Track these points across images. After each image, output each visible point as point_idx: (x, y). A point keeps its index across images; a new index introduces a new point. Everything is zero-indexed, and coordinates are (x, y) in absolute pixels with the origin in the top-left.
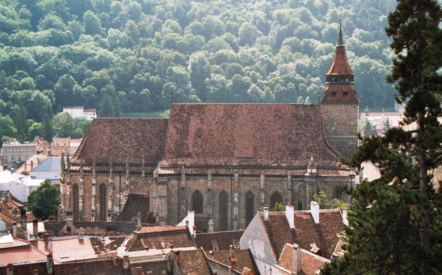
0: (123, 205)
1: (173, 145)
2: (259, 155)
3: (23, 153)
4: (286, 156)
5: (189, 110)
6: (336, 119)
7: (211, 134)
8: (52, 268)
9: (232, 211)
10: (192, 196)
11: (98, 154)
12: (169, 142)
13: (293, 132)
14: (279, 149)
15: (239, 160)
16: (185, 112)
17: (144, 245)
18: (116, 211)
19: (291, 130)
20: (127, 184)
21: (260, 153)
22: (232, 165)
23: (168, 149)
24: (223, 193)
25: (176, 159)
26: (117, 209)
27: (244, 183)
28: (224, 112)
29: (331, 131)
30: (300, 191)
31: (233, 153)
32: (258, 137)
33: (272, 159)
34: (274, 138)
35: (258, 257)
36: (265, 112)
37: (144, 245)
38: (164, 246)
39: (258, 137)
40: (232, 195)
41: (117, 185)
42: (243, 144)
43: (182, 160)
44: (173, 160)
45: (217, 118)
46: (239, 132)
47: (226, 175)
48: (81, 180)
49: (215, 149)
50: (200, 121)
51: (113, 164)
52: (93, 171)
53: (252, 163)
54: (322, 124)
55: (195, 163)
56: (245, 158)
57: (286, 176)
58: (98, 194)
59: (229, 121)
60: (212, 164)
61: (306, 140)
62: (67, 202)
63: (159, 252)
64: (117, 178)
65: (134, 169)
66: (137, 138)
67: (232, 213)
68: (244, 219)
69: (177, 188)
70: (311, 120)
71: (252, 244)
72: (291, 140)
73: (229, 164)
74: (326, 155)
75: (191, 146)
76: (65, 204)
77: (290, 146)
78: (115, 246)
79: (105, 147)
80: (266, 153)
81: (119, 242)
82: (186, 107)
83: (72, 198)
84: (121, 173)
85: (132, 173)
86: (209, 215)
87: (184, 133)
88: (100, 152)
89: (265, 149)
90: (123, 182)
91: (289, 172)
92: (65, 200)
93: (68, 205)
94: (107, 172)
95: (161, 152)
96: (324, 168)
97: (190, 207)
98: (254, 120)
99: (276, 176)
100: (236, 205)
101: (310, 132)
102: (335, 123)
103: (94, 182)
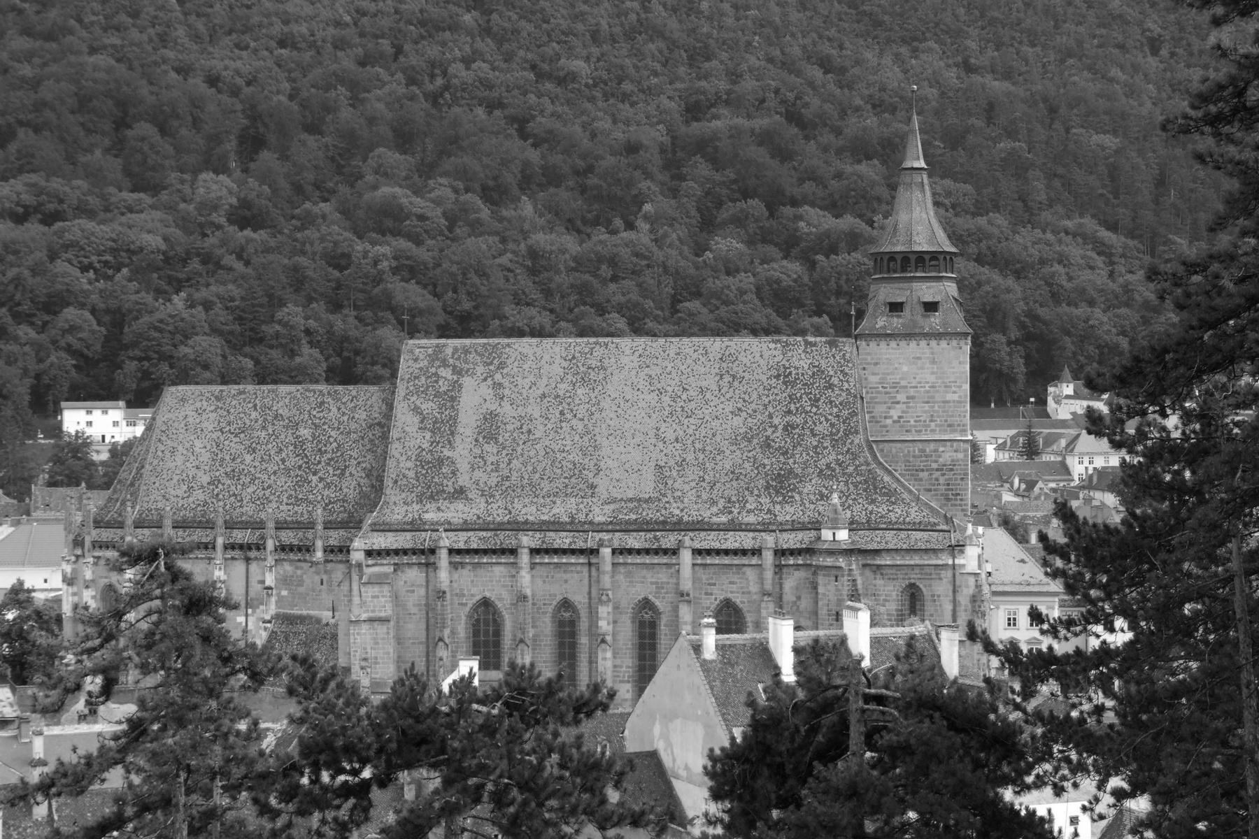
1: (409, 464)
2: (673, 490)
4: (756, 492)
6: (903, 383)
7: (525, 428)
9: (592, 662)
10: (470, 616)
11: (180, 492)
12: (397, 455)
13: (776, 421)
14: (733, 473)
15: (612, 507)
16: (445, 364)
19: (770, 416)
20: (268, 583)
21: (676, 485)
22: (591, 523)
23: (394, 476)
24: (566, 604)
25: (419, 507)
27: (629, 574)
28: (565, 364)
29: (889, 421)
30: (799, 598)
31: (593, 487)
32: (670, 436)
33: (714, 503)
34: (718, 438)
35: (683, 773)
36: (689, 361)
39: (670, 436)
43: (439, 509)
44: (410, 509)
45: (545, 381)
46: (611, 423)
47: (573, 552)
49: (537, 476)
50: (490, 391)
51: (225, 522)
53: (650, 514)
54: (862, 398)
55: (479, 518)
56: (631, 500)
57: (756, 552)
59: (580, 392)
60: (531, 518)
61: (815, 443)
64: (239, 567)
65: (288, 537)
66: (299, 444)
67: (590, 670)
68: (629, 686)
69: (423, 591)
71: (665, 736)
72: (769, 446)
73: (582, 517)
74: (875, 488)
75: (463, 466)
77: (766, 461)
79: (200, 474)
80: (693, 484)
82: (449, 351)
84: (250, 549)
85: (283, 548)
87: (443, 428)
88: (185, 488)
89: (692, 474)
91: (769, 540)
95: (373, 486)
96: (871, 526)
97: (465, 646)
98: (659, 386)
99: (727, 552)
100: (603, 641)
101: (827, 420)
102: (901, 397)
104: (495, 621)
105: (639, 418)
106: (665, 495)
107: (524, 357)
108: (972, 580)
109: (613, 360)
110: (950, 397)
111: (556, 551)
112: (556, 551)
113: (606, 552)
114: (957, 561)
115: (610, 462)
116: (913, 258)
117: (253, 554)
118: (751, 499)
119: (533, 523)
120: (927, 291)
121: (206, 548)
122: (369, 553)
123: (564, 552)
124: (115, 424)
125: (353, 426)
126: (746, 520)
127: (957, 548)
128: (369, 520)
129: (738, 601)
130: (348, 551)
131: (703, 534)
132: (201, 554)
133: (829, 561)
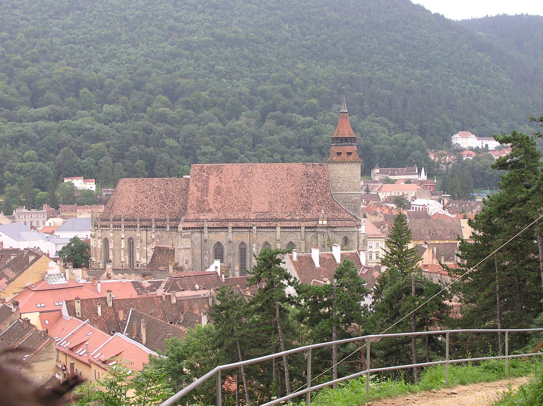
0: (150, 256)
1: (195, 202)
3: (35, 219)
5: (208, 170)
6: (341, 176)
8: (112, 301)
10: (214, 247)
11: (126, 211)
12: (191, 199)
13: (304, 188)
15: (256, 214)
17: (180, 287)
18: (143, 262)
21: (275, 208)
24: (243, 243)
26: (144, 261)
28: (241, 171)
29: (337, 188)
30: (312, 241)
31: (250, 208)
32: (273, 193)
33: (286, 213)
34: (287, 193)
37: (180, 287)
38: (198, 288)
39: (273, 193)
40: (251, 246)
41: (144, 239)
42: (259, 200)
45: (234, 176)
48: (111, 235)
50: (218, 179)
52: (122, 227)
53: (267, 216)
56: (262, 212)
58: (127, 247)
60: (232, 218)
62: (99, 255)
63: (194, 293)
64: (144, 233)
65: (159, 223)
66: (161, 196)
70: (320, 178)
74: (334, 208)
75: (211, 202)
76: (96, 257)
77: (302, 200)
78: (154, 288)
79: (131, 205)
81: (157, 285)
82: (205, 168)
83: (103, 251)
85: (157, 227)
86: (230, 264)
87: (204, 191)
88: (127, 209)
89: (280, 204)
90: (149, 236)
91: (303, 224)
92: (96, 253)
93: (99, 257)
94: (135, 227)
99: (291, 228)
101: (320, 188)
102: (341, 181)
103: (123, 236)
104: (221, 248)
105: (263, 188)
106: (272, 211)
107: (228, 169)
108: (363, 235)
109: (255, 170)
110: (355, 180)
111: (240, 228)
112: (240, 228)
113: (255, 228)
114: (359, 230)
115: (255, 201)
116: (344, 139)
117: (148, 229)
118: (297, 212)
119: (232, 220)
120: (348, 149)
121: (134, 227)
122: (184, 229)
123: (242, 228)
124: (80, 184)
125: (177, 190)
126: (296, 218)
127: (359, 226)
128: (183, 218)
129: (294, 242)
130: (177, 228)
131: (283, 222)
132: (133, 229)
133: (321, 230)
